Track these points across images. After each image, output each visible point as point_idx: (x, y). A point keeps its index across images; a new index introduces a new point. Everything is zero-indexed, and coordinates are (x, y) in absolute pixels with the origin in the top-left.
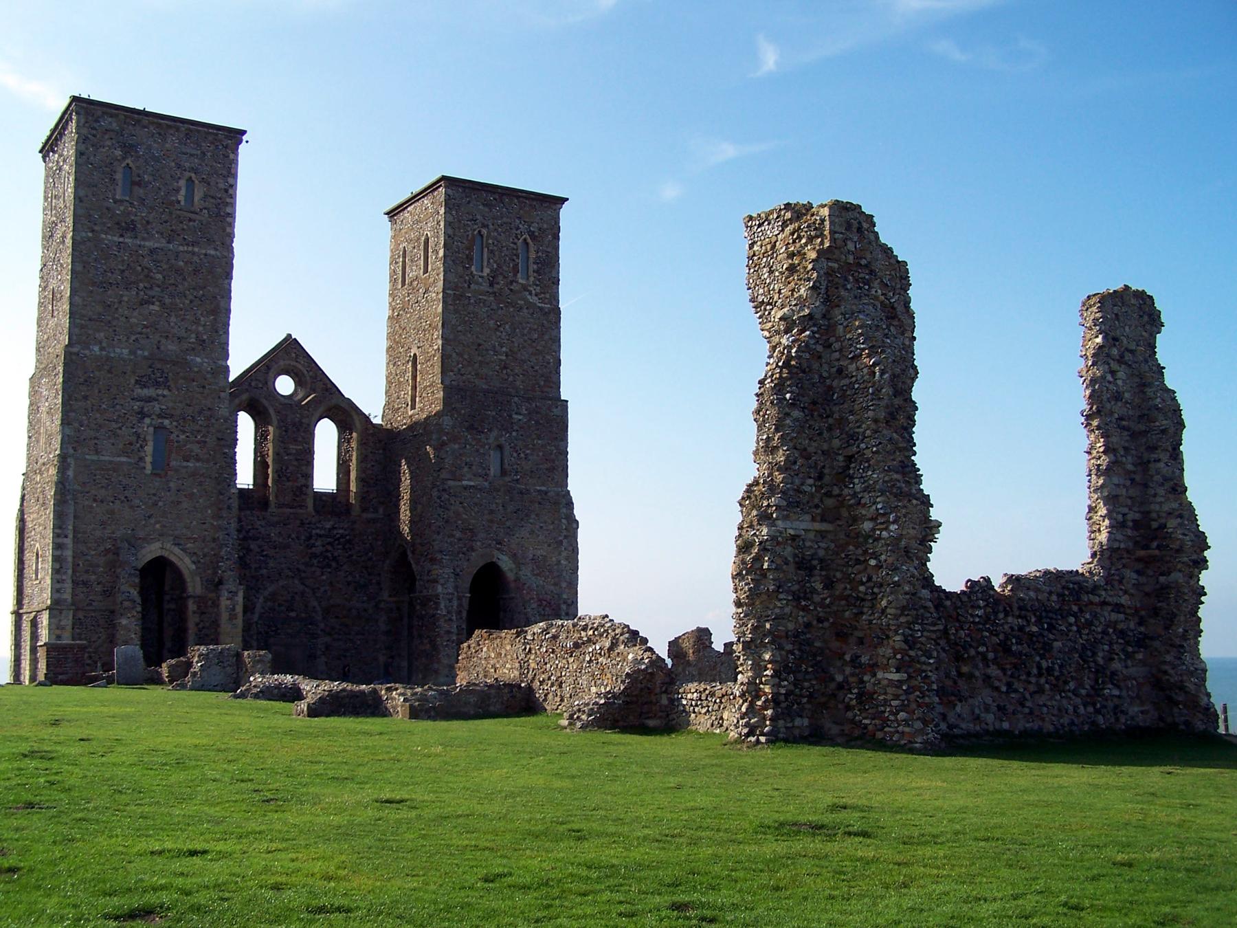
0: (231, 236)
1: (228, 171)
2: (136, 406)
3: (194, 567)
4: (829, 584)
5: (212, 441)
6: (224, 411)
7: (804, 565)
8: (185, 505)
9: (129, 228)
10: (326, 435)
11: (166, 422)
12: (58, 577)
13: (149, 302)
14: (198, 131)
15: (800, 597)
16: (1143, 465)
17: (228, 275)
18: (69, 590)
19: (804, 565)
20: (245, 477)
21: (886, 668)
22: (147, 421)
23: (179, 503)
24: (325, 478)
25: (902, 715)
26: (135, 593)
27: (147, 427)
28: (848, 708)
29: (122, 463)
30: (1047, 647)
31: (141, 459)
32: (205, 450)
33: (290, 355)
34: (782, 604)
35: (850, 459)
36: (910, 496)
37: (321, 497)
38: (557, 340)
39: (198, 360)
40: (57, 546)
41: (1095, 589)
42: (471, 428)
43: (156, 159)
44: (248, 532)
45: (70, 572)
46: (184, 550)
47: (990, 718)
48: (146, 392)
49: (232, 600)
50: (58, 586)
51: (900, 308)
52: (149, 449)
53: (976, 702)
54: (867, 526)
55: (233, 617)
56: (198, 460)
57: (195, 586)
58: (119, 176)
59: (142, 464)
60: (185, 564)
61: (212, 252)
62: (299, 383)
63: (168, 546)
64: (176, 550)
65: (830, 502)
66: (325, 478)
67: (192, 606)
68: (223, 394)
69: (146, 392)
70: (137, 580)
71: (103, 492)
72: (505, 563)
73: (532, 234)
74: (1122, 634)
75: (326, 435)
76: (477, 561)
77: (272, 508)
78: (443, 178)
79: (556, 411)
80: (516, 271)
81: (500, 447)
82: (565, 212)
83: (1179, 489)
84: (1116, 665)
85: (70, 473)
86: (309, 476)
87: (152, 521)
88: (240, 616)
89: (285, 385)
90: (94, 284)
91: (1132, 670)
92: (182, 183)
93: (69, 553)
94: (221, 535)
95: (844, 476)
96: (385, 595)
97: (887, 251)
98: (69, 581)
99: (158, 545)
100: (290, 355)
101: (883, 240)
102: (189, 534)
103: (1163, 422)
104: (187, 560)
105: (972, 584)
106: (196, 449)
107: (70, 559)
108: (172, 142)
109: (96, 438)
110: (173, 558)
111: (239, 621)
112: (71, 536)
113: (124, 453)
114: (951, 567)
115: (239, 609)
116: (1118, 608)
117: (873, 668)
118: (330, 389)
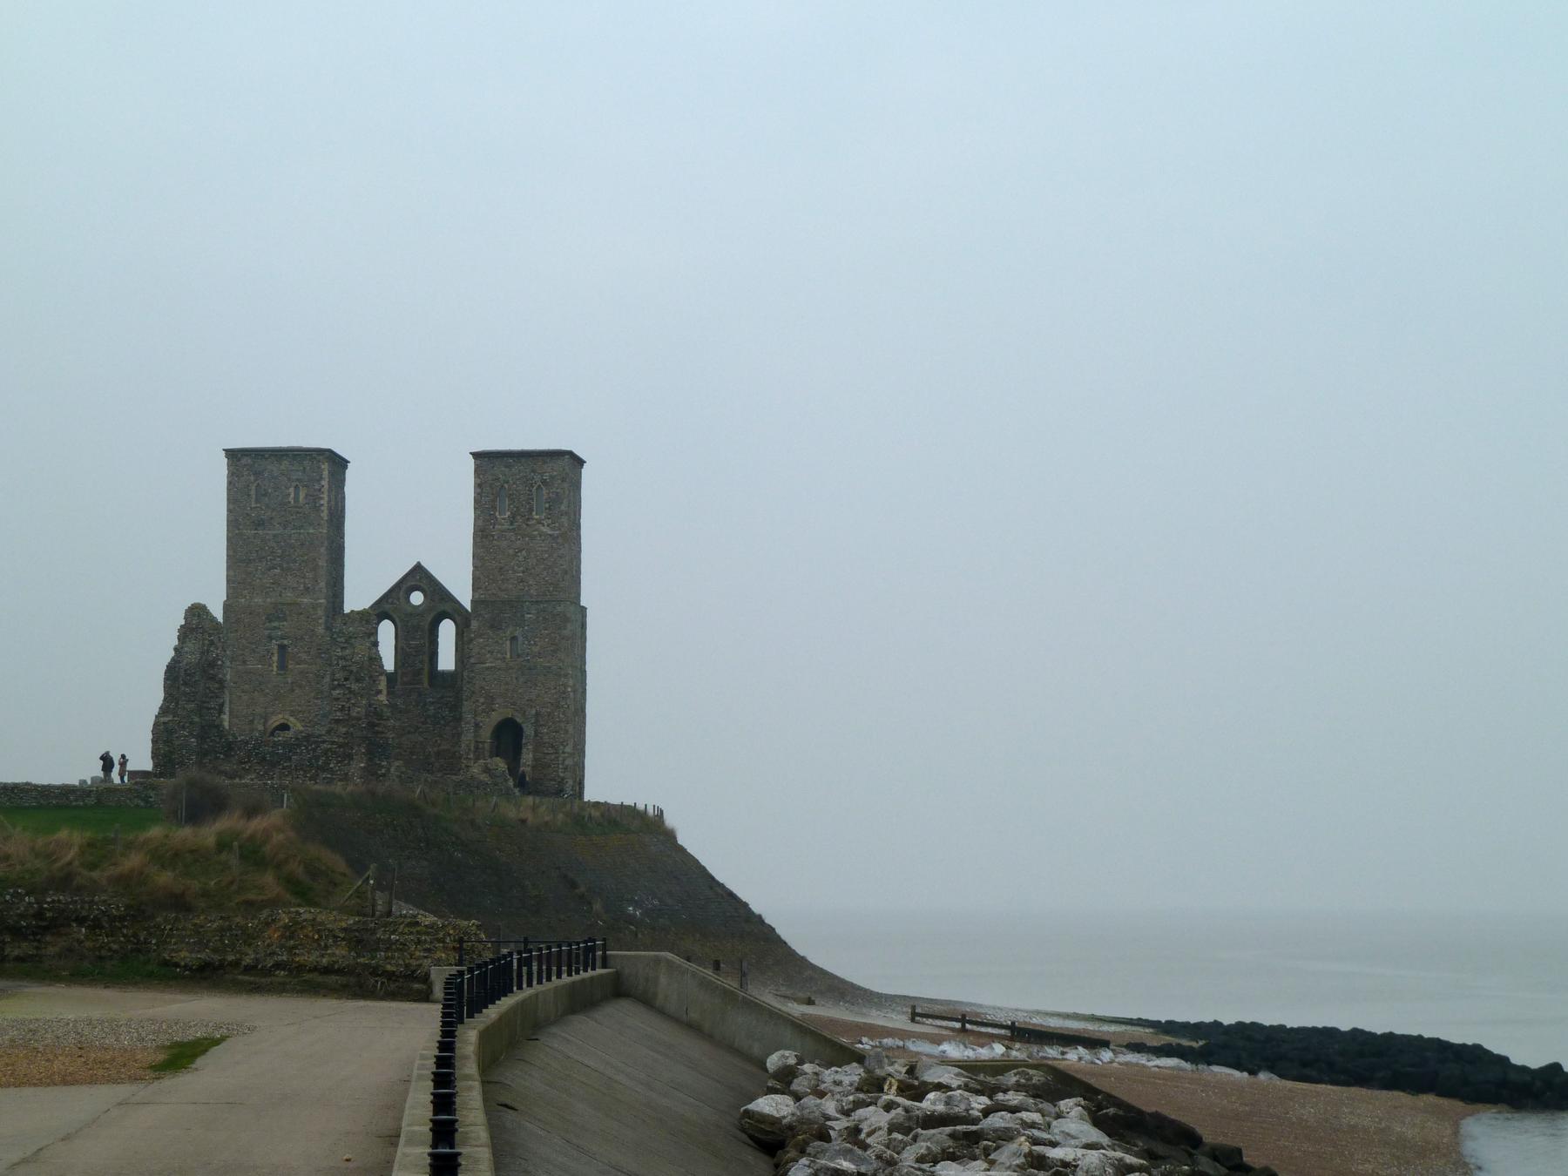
9: (259, 524)
10: (447, 631)
20: (389, 664)
24: (447, 660)
27: (274, 645)
30: (290, 759)
33: (418, 577)
37: (444, 673)
42: (492, 627)
52: (275, 658)
58: (253, 492)
66: (447, 660)
73: (544, 482)
75: (447, 631)
76: (496, 717)
80: (531, 510)
81: (514, 639)
89: (417, 598)
92: (292, 490)
100: (418, 577)
106: (304, 656)
108: (285, 464)
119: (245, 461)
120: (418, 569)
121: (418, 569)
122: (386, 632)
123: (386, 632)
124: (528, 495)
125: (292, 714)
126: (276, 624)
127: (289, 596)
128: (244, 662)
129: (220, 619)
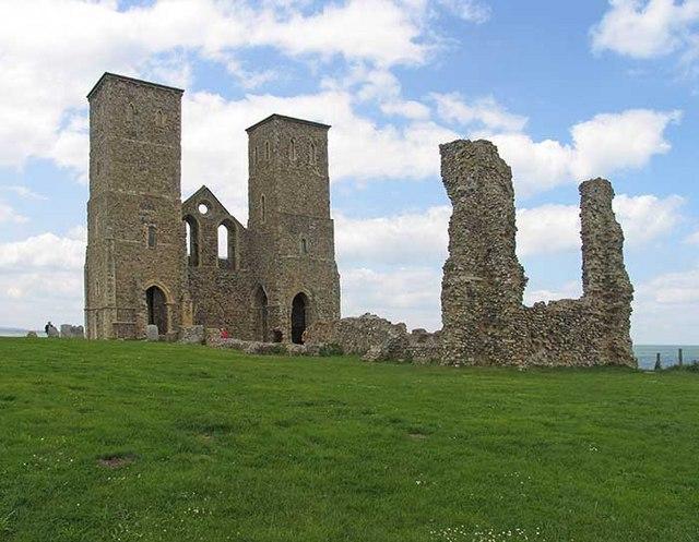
0: (180, 139)
1: (178, 110)
2: (141, 217)
4: (481, 304)
5: (175, 234)
6: (180, 219)
7: (470, 294)
10: (223, 232)
15: (470, 308)
16: (607, 255)
17: (179, 158)
19: (470, 294)
20: (189, 252)
21: (507, 338)
24: (223, 253)
25: (513, 357)
26: (145, 303)
27: (145, 227)
28: (490, 354)
33: (204, 195)
34: (463, 312)
35: (489, 251)
36: (516, 267)
38: (328, 192)
41: (587, 308)
47: (545, 360)
49: (188, 308)
51: (508, 187)
53: (539, 354)
54: (497, 279)
55: (188, 313)
57: (171, 300)
60: (166, 290)
62: (209, 208)
65: (482, 269)
66: (223, 253)
67: (169, 308)
70: (145, 296)
72: (308, 294)
74: (597, 327)
75: (223, 232)
76: (294, 292)
77: (200, 265)
78: (274, 117)
79: (329, 225)
82: (329, 132)
83: (621, 266)
84: (595, 340)
85: (112, 247)
86: (216, 251)
89: (203, 209)
91: (603, 343)
93: (113, 283)
94: (182, 277)
95: (486, 258)
96: (252, 306)
97: (503, 162)
100: (204, 195)
101: (501, 156)
103: (615, 237)
105: (536, 305)
114: (529, 299)
116: (596, 316)
117: (500, 338)
118: (224, 211)
119: (121, 85)
120: (205, 190)
121: (205, 190)
124: (288, 153)
127: (155, 192)
129: (183, 199)
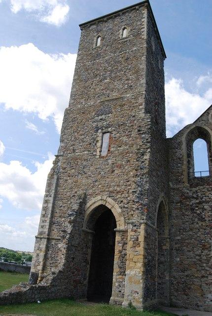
2: (94, 125)
3: (120, 210)
8: (116, 172)
11: (109, 129)
12: (43, 219)
13: (105, 78)
14: (127, 11)
18: (48, 227)
22: (100, 131)
23: (113, 171)
29: (84, 155)
31: (95, 151)
32: (131, 139)
39: (128, 95)
40: (46, 202)
43: (110, 29)
44: (202, 199)
45: (49, 216)
46: (115, 200)
48: (100, 117)
50: (43, 224)
56: (126, 145)
57: (121, 226)
59: (94, 154)
60: (116, 211)
61: (135, 48)
63: (105, 197)
64: (110, 200)
68: (141, 107)
69: (100, 117)
71: (73, 171)
87: (96, 184)
88: (142, 244)
90: (81, 81)
93: (50, 205)
98: (48, 221)
99: (99, 197)
102: (118, 189)
104: (117, 206)
107: (50, 209)
108: (117, 20)
109: (74, 145)
110: (109, 207)
111: (141, 249)
112: (53, 196)
113: (86, 149)
115: (141, 239)
122: (200, 147)
123: (200, 147)
125: (111, 194)
126: (103, 117)
127: (115, 95)
128: (74, 151)
